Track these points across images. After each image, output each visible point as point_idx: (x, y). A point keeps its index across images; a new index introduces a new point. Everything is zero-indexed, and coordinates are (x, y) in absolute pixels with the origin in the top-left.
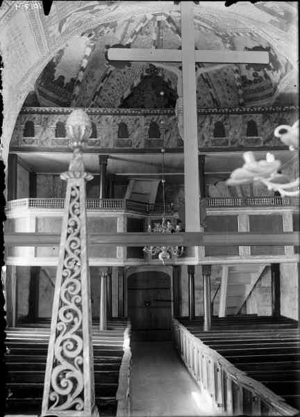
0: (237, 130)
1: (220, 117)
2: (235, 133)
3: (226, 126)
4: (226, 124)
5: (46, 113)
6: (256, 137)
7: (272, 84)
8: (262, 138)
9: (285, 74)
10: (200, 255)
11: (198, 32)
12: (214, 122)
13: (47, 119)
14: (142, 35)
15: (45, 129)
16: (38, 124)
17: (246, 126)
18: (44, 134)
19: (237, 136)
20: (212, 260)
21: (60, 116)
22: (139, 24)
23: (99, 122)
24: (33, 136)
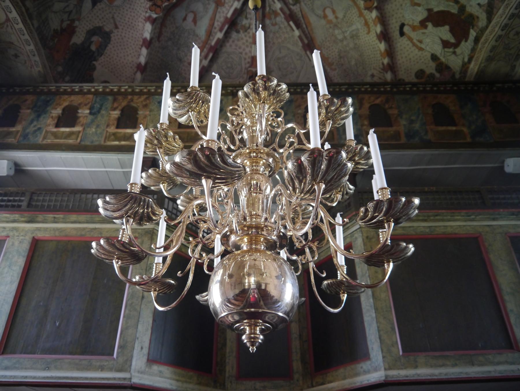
0: (413, 118)
1: (377, 98)
2: (412, 122)
3: (390, 112)
4: (391, 108)
5: (50, 93)
6: (454, 128)
7: (454, 75)
8: (465, 130)
9: (487, 27)
10: (386, 350)
11: (323, 22)
12: (367, 105)
13: (48, 101)
14: (238, 32)
15: (39, 116)
16: (28, 108)
17: (430, 111)
18: (35, 123)
19: (417, 126)
20: (427, 365)
21: (73, 98)
22: (232, 5)
23: (146, 106)
24: (13, 126)
